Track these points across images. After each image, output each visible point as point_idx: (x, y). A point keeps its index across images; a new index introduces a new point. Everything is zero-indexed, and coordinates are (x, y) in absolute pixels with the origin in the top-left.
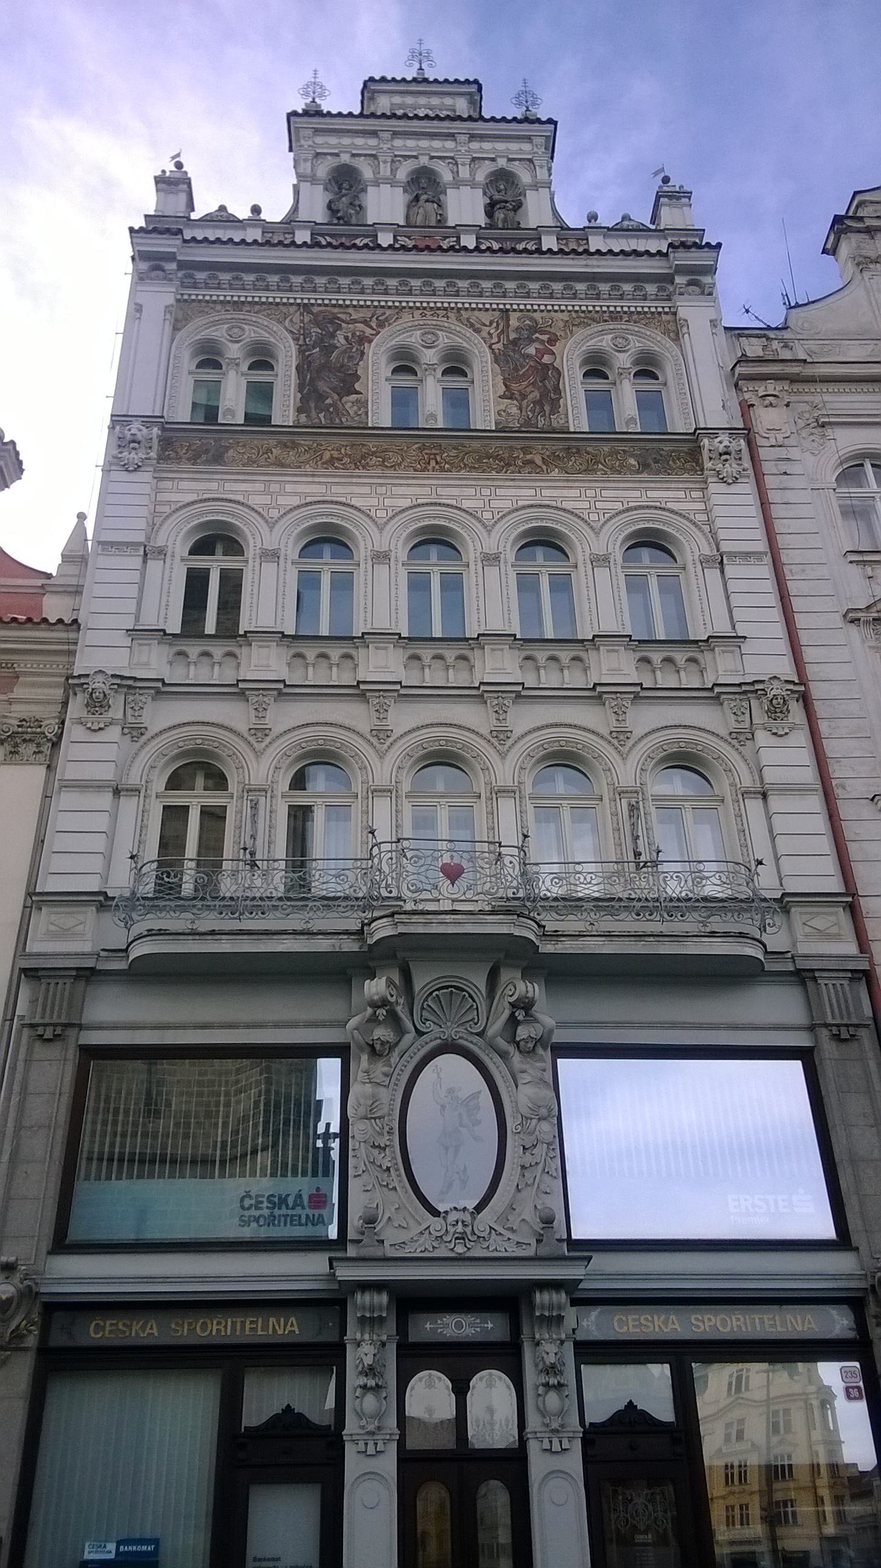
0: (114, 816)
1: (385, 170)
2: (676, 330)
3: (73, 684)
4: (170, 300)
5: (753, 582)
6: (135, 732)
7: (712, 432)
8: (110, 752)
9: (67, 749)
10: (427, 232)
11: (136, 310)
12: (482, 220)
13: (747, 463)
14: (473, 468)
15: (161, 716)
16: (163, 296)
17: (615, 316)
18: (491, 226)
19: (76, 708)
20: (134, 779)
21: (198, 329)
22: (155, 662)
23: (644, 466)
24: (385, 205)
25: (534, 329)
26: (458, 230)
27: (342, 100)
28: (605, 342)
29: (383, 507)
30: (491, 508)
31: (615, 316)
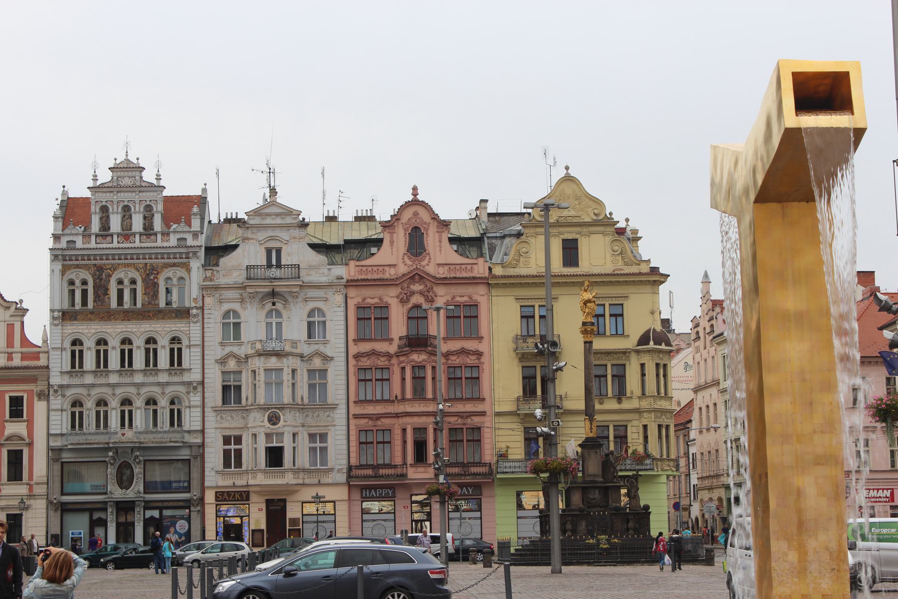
1: (115, 210)
4: (60, 267)
7: (192, 308)
10: (127, 234)
11: (52, 271)
12: (142, 230)
13: (200, 318)
14: (135, 319)
16: (58, 266)
17: (174, 265)
23: (176, 317)
30: (139, 331)
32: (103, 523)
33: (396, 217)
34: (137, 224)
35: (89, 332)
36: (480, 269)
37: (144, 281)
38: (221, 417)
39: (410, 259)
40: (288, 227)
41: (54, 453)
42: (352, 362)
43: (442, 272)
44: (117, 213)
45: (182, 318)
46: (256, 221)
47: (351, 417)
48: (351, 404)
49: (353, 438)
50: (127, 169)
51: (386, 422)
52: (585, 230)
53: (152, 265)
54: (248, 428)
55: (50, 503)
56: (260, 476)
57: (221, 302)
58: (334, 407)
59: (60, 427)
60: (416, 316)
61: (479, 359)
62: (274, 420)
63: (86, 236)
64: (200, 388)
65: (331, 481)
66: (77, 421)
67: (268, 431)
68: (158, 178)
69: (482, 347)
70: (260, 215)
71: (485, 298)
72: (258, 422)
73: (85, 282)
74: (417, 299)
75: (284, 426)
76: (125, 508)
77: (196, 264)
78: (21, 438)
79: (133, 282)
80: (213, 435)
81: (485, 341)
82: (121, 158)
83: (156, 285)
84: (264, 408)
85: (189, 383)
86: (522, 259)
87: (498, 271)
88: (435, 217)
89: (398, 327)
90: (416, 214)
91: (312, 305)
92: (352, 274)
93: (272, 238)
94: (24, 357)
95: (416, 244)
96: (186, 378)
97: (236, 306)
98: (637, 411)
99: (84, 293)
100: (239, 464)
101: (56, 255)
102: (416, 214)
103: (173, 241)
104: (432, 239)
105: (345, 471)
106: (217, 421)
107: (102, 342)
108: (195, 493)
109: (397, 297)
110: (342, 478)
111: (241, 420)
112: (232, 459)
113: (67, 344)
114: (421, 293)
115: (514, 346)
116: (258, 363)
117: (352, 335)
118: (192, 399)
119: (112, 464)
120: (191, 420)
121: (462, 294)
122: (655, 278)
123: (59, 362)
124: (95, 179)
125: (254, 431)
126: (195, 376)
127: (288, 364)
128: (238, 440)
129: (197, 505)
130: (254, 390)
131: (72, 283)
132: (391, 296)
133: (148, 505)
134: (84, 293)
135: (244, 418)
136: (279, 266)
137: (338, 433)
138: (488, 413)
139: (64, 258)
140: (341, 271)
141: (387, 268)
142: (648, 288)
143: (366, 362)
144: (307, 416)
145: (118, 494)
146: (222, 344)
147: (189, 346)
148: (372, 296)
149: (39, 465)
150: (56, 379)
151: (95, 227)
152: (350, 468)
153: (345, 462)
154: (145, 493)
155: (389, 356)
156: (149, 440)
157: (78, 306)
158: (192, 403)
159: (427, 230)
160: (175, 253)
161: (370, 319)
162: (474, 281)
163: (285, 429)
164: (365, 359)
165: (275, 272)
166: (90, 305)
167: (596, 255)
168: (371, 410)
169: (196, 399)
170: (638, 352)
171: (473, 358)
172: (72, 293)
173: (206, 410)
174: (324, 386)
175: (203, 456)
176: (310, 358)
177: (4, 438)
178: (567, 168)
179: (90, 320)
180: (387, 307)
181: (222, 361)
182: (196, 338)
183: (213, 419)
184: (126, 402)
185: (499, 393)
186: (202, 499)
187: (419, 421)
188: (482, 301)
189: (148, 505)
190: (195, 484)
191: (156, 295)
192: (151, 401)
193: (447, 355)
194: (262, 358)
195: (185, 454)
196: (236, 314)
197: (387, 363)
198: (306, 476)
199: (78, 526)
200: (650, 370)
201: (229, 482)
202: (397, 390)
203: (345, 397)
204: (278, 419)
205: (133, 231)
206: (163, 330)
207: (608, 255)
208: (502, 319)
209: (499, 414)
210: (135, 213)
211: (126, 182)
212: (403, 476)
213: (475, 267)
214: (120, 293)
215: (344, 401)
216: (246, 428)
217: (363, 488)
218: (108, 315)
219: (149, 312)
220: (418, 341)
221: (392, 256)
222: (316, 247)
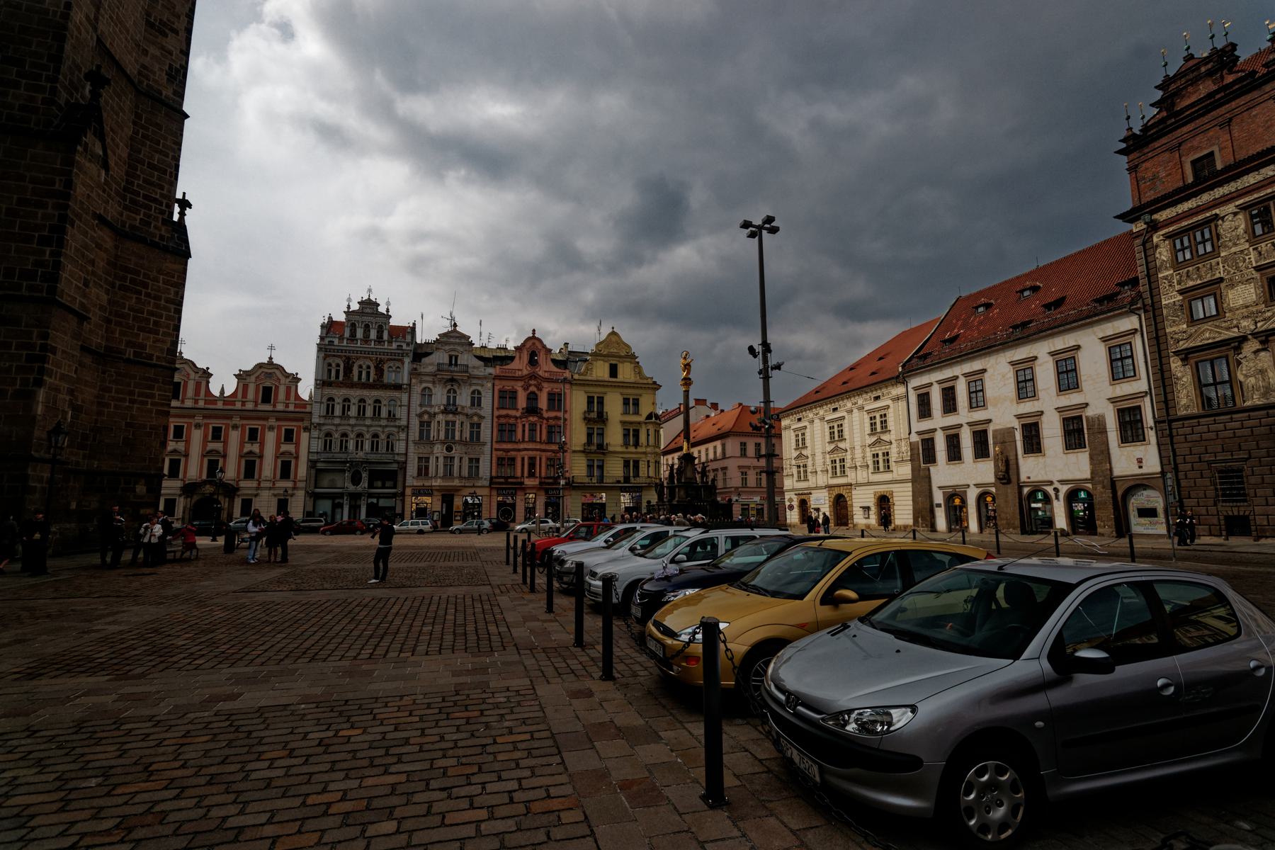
2: (403, 363)
5: (405, 409)
10: (366, 339)
29: (355, 394)
32: (341, 506)
33: (523, 345)
34: (373, 334)
36: (567, 374)
40: (461, 344)
41: (312, 464)
43: (547, 375)
50: (369, 306)
55: (307, 492)
57: (421, 382)
58: (484, 444)
60: (532, 398)
62: (449, 449)
63: (341, 338)
66: (327, 446)
68: (388, 310)
69: (567, 416)
72: (439, 450)
73: (338, 365)
74: (532, 389)
76: (355, 497)
77: (407, 360)
79: (369, 367)
84: (443, 443)
87: (576, 377)
88: (544, 346)
89: (522, 402)
91: (474, 388)
95: (533, 362)
97: (430, 385)
98: (645, 453)
99: (338, 372)
100: (427, 474)
101: (321, 348)
103: (394, 346)
104: (541, 358)
108: (399, 490)
112: (423, 471)
116: (440, 417)
120: (400, 447)
122: (655, 387)
123: (317, 412)
124: (349, 307)
126: (404, 423)
127: (458, 419)
128: (427, 459)
130: (437, 430)
131: (330, 365)
132: (518, 386)
133: (370, 496)
134: (338, 372)
136: (456, 364)
139: (324, 349)
140: (490, 370)
143: (503, 421)
145: (352, 488)
146: (421, 405)
148: (508, 385)
149: (302, 470)
150: (316, 420)
151: (347, 334)
152: (492, 478)
155: (516, 418)
156: (373, 457)
157: (333, 378)
161: (507, 398)
162: (565, 381)
165: (453, 368)
166: (341, 378)
167: (626, 373)
168: (505, 446)
169: (403, 436)
172: (330, 371)
174: (478, 433)
180: (515, 392)
181: (420, 415)
182: (405, 402)
184: (360, 435)
185: (575, 441)
186: (403, 494)
187: (532, 453)
189: (370, 496)
190: (400, 484)
192: (376, 436)
193: (548, 419)
195: (394, 467)
199: (325, 506)
200: (652, 432)
201: (420, 484)
202: (519, 436)
208: (577, 402)
211: (368, 310)
212: (522, 483)
214: (360, 373)
216: (432, 453)
217: (498, 489)
218: (352, 386)
220: (532, 410)
221: (520, 366)
222: (480, 358)
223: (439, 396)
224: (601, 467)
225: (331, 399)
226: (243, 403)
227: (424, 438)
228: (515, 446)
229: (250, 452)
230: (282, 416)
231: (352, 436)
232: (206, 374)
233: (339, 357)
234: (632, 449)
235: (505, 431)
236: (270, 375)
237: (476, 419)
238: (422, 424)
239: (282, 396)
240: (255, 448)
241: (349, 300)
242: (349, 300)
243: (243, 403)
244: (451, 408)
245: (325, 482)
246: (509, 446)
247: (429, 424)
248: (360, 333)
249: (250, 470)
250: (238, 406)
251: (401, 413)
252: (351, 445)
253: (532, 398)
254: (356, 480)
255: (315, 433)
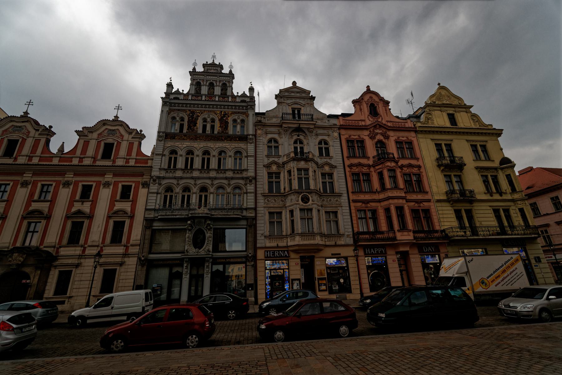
0: (157, 197)
1: (205, 83)
3: (152, 177)
6: (160, 184)
7: (249, 135)
8: (156, 188)
9: (151, 187)
10: (211, 95)
15: (164, 182)
17: (239, 113)
18: (222, 94)
19: (152, 181)
20: (160, 192)
21: (173, 114)
22: (163, 174)
23: (239, 140)
24: (204, 90)
25: (226, 114)
26: (215, 96)
27: (200, 69)
28: (236, 117)
31: (239, 113)
35: (182, 146)
37: (219, 120)
38: (268, 200)
39: (372, 118)
40: (304, 98)
41: (148, 223)
42: (348, 169)
44: (206, 85)
45: (242, 141)
46: (286, 94)
47: (351, 201)
48: (350, 194)
49: (354, 215)
51: (373, 204)
52: (457, 109)
53: (225, 112)
54: (286, 207)
55: (139, 259)
56: (297, 238)
58: (340, 195)
59: (154, 204)
60: (381, 145)
61: (419, 170)
62: (305, 200)
64: (253, 181)
65: (343, 243)
66: (168, 202)
67: (302, 207)
69: (420, 163)
70: (288, 92)
71: (415, 138)
72: (295, 202)
73: (182, 119)
74: (379, 137)
75: (312, 204)
76: (197, 263)
78: (125, 212)
79: (213, 121)
80: (263, 212)
81: (420, 160)
82: (210, 62)
83: (227, 123)
85: (247, 178)
86: (430, 121)
88: (382, 99)
89: (371, 151)
90: (371, 97)
91: (320, 138)
92: (342, 123)
93: (296, 103)
94: (137, 161)
96: (244, 175)
98: (513, 201)
102: (371, 97)
105: (351, 236)
106: (265, 203)
107: (190, 152)
109: (368, 136)
110: (350, 241)
111: (281, 203)
113: (167, 152)
114: (381, 134)
115: (437, 164)
116: (293, 165)
117: (346, 154)
118: (248, 188)
119: (190, 230)
121: (403, 136)
124: (194, 69)
125: (291, 208)
126: (251, 174)
127: (311, 166)
129: (252, 261)
135: (283, 201)
137: (344, 211)
138: (432, 201)
141: (360, 122)
142: (494, 138)
143: (355, 170)
144: (323, 200)
145: (192, 251)
146: (268, 156)
147: (247, 157)
148: (355, 135)
149: (137, 232)
150: (155, 173)
153: (351, 230)
154: (213, 252)
155: (369, 166)
158: (248, 191)
159: (378, 105)
160: (239, 106)
162: (408, 130)
163: (313, 206)
164: (355, 168)
166: (185, 131)
168: (362, 197)
170: (502, 169)
171: (416, 169)
173: (258, 195)
175: (255, 226)
176: (322, 166)
177: (112, 212)
178: (439, 84)
179: (184, 139)
183: (263, 201)
184: (204, 189)
185: (435, 189)
188: (414, 140)
189: (215, 261)
191: (226, 128)
194: (295, 162)
196: (276, 141)
197: (368, 170)
198: (326, 240)
201: (274, 244)
202: (376, 185)
203: (345, 189)
204: (308, 200)
205: (215, 94)
206: (230, 146)
207: (472, 122)
208: (426, 150)
209: (438, 201)
210: (217, 86)
212: (395, 239)
213: (406, 124)
214: (204, 127)
215: (346, 192)
216: (285, 207)
217: (364, 247)
218: (196, 137)
219: (222, 137)
223: (286, 146)
224: (471, 218)
225: (173, 152)
226: (81, 159)
227: (274, 189)
228: (376, 197)
229: (79, 212)
230: (119, 172)
231: (195, 190)
232: (49, 132)
233: (184, 111)
234: (497, 197)
235: (359, 179)
236: (112, 132)
237: (327, 168)
238: (270, 175)
239: (123, 152)
240: (86, 207)
241: (195, 64)
242: (195, 64)
243: (81, 159)
244: (300, 155)
245: (166, 246)
246: (367, 197)
247: (278, 175)
248: (204, 90)
249: (76, 231)
250: (75, 161)
251: (248, 164)
252: (194, 199)
253: (381, 145)
254: (198, 242)
255: (154, 188)
